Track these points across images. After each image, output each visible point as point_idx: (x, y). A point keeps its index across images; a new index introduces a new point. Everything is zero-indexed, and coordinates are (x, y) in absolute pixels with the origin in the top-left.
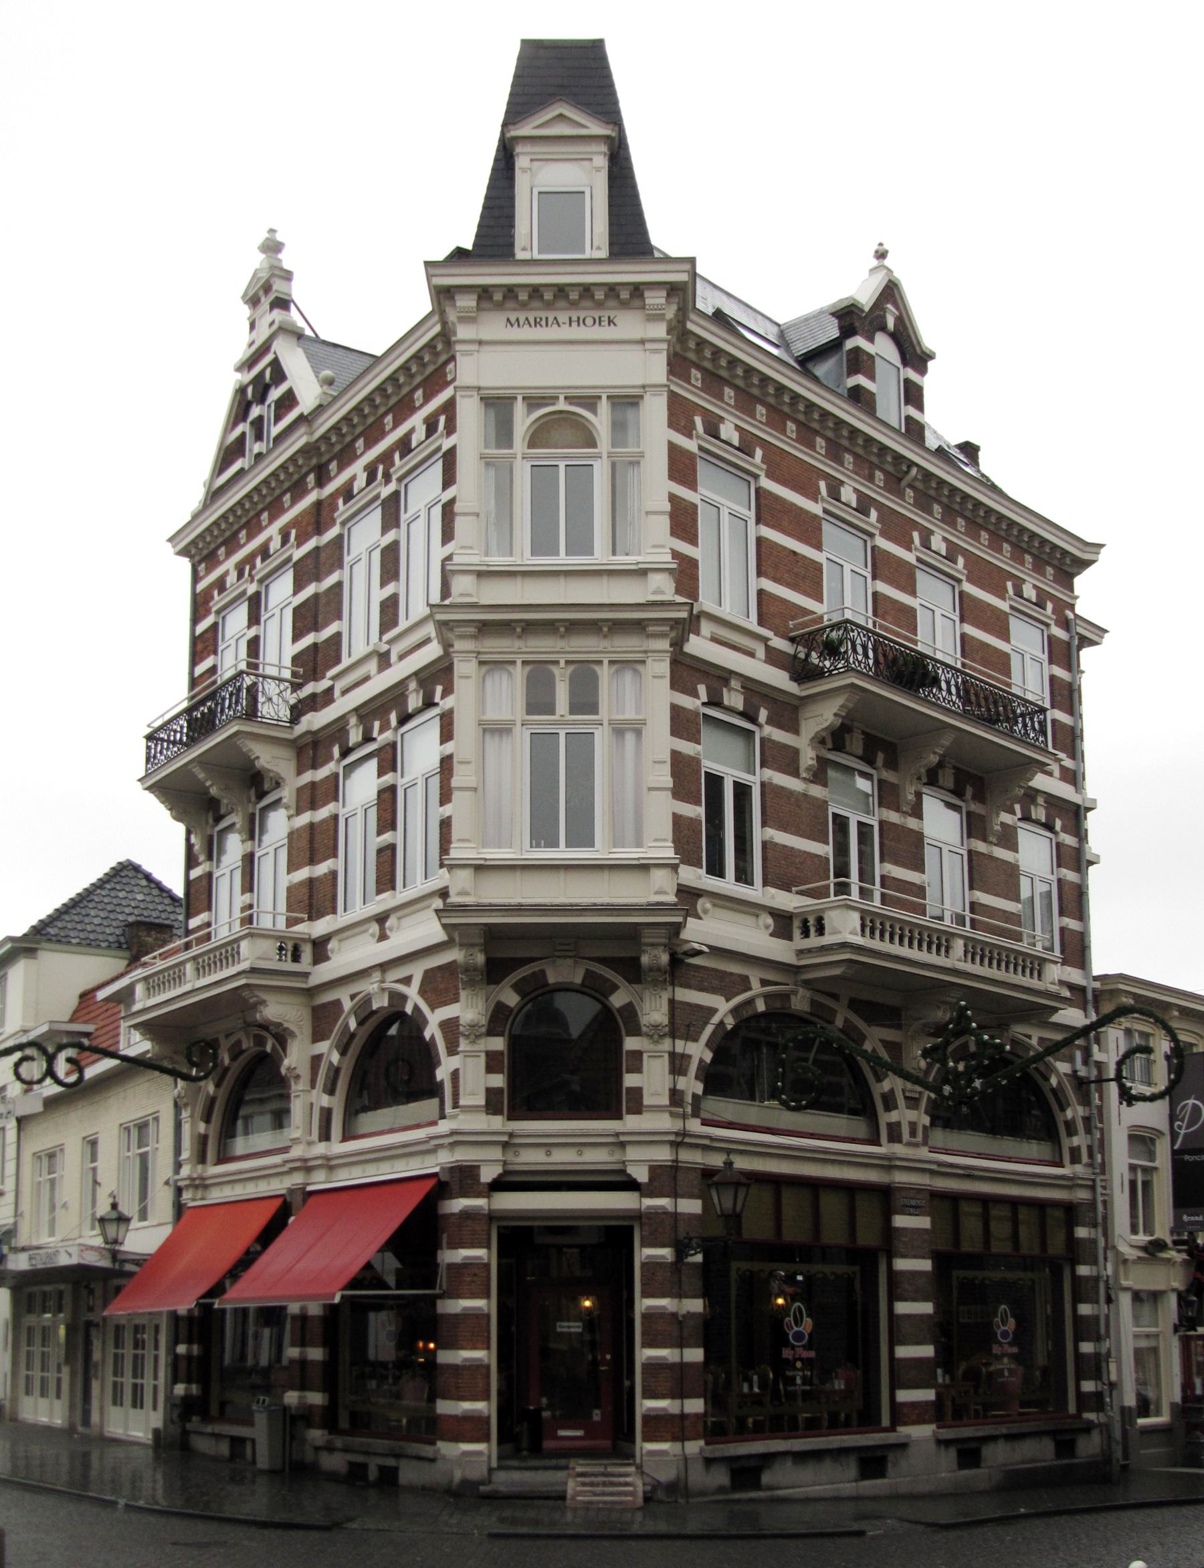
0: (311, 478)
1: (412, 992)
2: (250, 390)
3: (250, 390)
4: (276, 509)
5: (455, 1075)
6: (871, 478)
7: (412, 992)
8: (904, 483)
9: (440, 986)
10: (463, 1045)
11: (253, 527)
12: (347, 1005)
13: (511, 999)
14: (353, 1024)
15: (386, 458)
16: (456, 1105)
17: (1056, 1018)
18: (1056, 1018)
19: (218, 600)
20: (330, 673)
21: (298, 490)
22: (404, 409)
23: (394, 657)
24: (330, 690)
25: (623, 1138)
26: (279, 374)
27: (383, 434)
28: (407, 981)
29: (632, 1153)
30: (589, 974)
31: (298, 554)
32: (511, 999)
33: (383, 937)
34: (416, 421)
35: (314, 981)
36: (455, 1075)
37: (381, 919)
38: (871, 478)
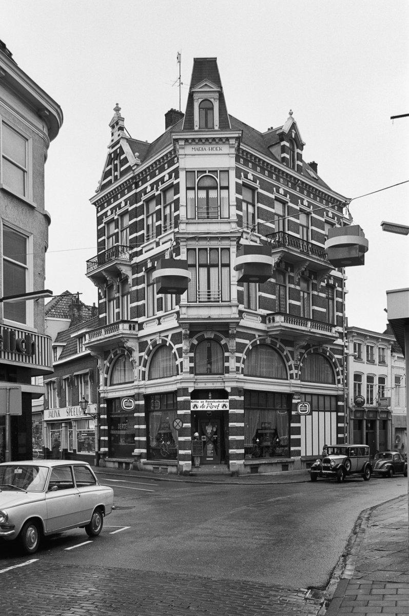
0: (134, 186)
1: (169, 340)
2: (113, 155)
3: (113, 155)
4: (123, 195)
5: (181, 363)
6: (287, 185)
7: (169, 340)
8: (297, 185)
9: (177, 338)
10: (184, 355)
11: (116, 199)
12: (149, 342)
13: (196, 342)
14: (151, 348)
15: (156, 183)
16: (182, 371)
17: (335, 342)
18: (335, 342)
19: (105, 220)
20: (142, 246)
21: (130, 190)
22: (162, 170)
23: (161, 243)
24: (142, 250)
25: (224, 380)
26: (122, 152)
27: (155, 176)
28: (167, 336)
29: (227, 384)
30: (215, 335)
31: (130, 209)
32: (196, 342)
33: (159, 324)
34: (165, 173)
35: (139, 336)
36: (181, 363)
37: (159, 319)
38: (287, 185)
